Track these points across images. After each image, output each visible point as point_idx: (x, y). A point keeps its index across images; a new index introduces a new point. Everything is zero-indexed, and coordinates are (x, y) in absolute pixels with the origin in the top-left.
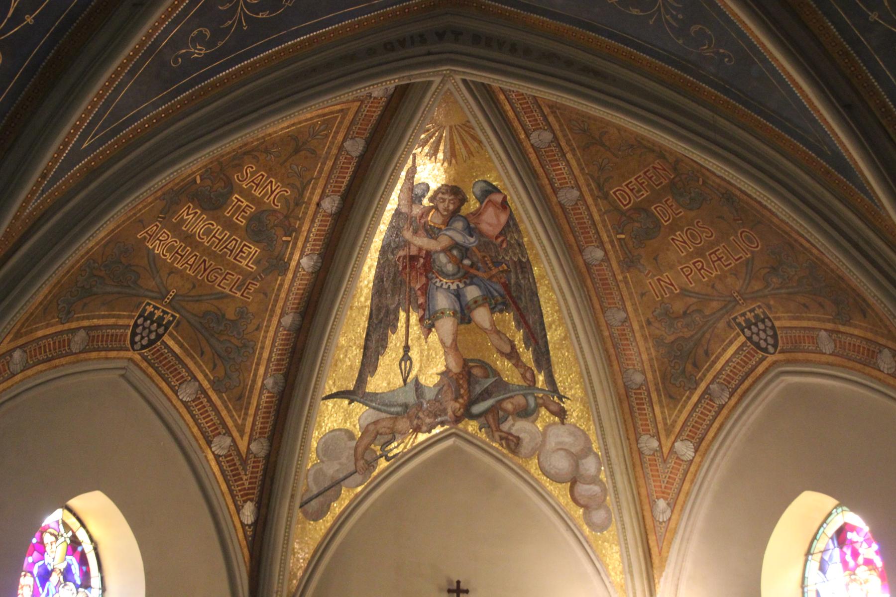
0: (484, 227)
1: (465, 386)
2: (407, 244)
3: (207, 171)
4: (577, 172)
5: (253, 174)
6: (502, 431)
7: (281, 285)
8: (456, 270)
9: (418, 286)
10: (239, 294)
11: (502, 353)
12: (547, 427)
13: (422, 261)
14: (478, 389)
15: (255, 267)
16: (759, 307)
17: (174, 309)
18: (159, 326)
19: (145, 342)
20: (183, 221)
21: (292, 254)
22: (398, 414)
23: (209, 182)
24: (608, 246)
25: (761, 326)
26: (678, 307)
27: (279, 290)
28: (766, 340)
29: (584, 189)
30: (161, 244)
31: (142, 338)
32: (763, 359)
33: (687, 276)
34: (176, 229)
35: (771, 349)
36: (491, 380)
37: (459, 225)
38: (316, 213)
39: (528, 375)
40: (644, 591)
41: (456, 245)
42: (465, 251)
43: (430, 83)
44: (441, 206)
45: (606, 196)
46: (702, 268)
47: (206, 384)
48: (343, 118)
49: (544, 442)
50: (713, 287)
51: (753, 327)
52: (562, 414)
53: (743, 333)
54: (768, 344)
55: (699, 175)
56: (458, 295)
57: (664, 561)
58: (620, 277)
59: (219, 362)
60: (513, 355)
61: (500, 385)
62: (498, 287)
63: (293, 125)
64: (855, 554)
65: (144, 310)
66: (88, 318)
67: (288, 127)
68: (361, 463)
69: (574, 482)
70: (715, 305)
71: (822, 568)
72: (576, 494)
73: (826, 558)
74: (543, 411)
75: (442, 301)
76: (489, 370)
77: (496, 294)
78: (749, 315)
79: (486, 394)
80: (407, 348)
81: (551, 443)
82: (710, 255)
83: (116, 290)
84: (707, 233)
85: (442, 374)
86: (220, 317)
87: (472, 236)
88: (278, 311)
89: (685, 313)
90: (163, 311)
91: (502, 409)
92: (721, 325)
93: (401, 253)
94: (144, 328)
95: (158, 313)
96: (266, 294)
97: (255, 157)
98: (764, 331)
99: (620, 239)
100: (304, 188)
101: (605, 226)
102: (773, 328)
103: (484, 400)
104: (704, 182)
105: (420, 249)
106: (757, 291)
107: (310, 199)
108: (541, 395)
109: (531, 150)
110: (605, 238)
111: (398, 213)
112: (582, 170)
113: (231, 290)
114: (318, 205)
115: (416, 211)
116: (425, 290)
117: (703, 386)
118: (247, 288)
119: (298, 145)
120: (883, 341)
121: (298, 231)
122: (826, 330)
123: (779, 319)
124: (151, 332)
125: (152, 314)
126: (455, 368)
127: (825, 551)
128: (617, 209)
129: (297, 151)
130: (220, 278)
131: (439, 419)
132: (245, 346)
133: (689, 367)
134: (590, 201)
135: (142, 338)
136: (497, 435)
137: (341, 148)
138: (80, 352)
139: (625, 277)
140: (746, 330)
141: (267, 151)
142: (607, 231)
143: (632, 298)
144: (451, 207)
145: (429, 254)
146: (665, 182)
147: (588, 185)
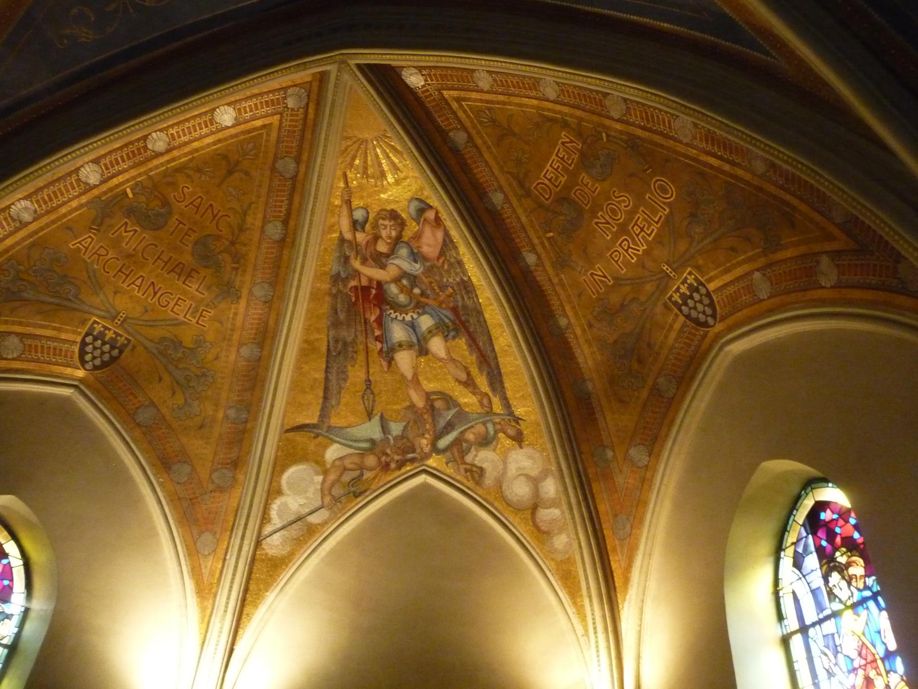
0: (426, 250)
1: (430, 420)
2: (357, 274)
3: (137, 184)
6: (466, 464)
7: (236, 314)
8: (408, 300)
9: (373, 318)
10: (194, 321)
11: (460, 382)
13: (374, 292)
14: (442, 423)
15: (206, 294)
16: (690, 273)
17: (129, 333)
18: (113, 347)
19: (98, 362)
25: (696, 296)
26: (615, 299)
31: (94, 358)
33: (616, 262)
35: (710, 321)
37: (404, 251)
39: (485, 401)
40: (604, 616)
41: (405, 274)
42: (414, 280)
45: (528, 194)
46: (629, 247)
49: (505, 472)
50: (643, 267)
51: (689, 301)
53: (681, 311)
54: (707, 316)
55: (600, 129)
57: (627, 580)
58: (555, 281)
60: (469, 383)
61: (462, 415)
62: (449, 313)
63: (219, 141)
64: (831, 537)
65: (92, 329)
66: (20, 324)
67: (214, 143)
68: (327, 499)
69: (534, 508)
70: (649, 288)
71: (798, 563)
72: (538, 520)
73: (800, 550)
74: (501, 435)
75: (398, 333)
76: (450, 401)
77: (447, 321)
78: (684, 289)
79: (449, 427)
80: (368, 382)
81: (512, 469)
82: (633, 228)
84: (624, 201)
86: (177, 344)
87: (416, 262)
89: (622, 305)
91: (466, 441)
92: (659, 309)
93: (353, 283)
94: (95, 348)
95: (109, 335)
96: (221, 322)
97: (188, 176)
98: (701, 302)
99: (549, 238)
102: (708, 295)
103: (448, 433)
104: (608, 136)
105: (370, 280)
106: (685, 252)
110: (536, 241)
113: (185, 317)
116: (380, 321)
117: (650, 382)
118: (201, 315)
122: (757, 270)
123: (710, 280)
127: (799, 540)
128: (541, 206)
129: (230, 173)
130: (172, 304)
131: (410, 456)
132: (204, 375)
133: (635, 366)
135: (94, 358)
138: (13, 359)
139: (561, 280)
140: (683, 308)
141: (199, 170)
144: (394, 234)
145: (380, 284)
147: (510, 185)
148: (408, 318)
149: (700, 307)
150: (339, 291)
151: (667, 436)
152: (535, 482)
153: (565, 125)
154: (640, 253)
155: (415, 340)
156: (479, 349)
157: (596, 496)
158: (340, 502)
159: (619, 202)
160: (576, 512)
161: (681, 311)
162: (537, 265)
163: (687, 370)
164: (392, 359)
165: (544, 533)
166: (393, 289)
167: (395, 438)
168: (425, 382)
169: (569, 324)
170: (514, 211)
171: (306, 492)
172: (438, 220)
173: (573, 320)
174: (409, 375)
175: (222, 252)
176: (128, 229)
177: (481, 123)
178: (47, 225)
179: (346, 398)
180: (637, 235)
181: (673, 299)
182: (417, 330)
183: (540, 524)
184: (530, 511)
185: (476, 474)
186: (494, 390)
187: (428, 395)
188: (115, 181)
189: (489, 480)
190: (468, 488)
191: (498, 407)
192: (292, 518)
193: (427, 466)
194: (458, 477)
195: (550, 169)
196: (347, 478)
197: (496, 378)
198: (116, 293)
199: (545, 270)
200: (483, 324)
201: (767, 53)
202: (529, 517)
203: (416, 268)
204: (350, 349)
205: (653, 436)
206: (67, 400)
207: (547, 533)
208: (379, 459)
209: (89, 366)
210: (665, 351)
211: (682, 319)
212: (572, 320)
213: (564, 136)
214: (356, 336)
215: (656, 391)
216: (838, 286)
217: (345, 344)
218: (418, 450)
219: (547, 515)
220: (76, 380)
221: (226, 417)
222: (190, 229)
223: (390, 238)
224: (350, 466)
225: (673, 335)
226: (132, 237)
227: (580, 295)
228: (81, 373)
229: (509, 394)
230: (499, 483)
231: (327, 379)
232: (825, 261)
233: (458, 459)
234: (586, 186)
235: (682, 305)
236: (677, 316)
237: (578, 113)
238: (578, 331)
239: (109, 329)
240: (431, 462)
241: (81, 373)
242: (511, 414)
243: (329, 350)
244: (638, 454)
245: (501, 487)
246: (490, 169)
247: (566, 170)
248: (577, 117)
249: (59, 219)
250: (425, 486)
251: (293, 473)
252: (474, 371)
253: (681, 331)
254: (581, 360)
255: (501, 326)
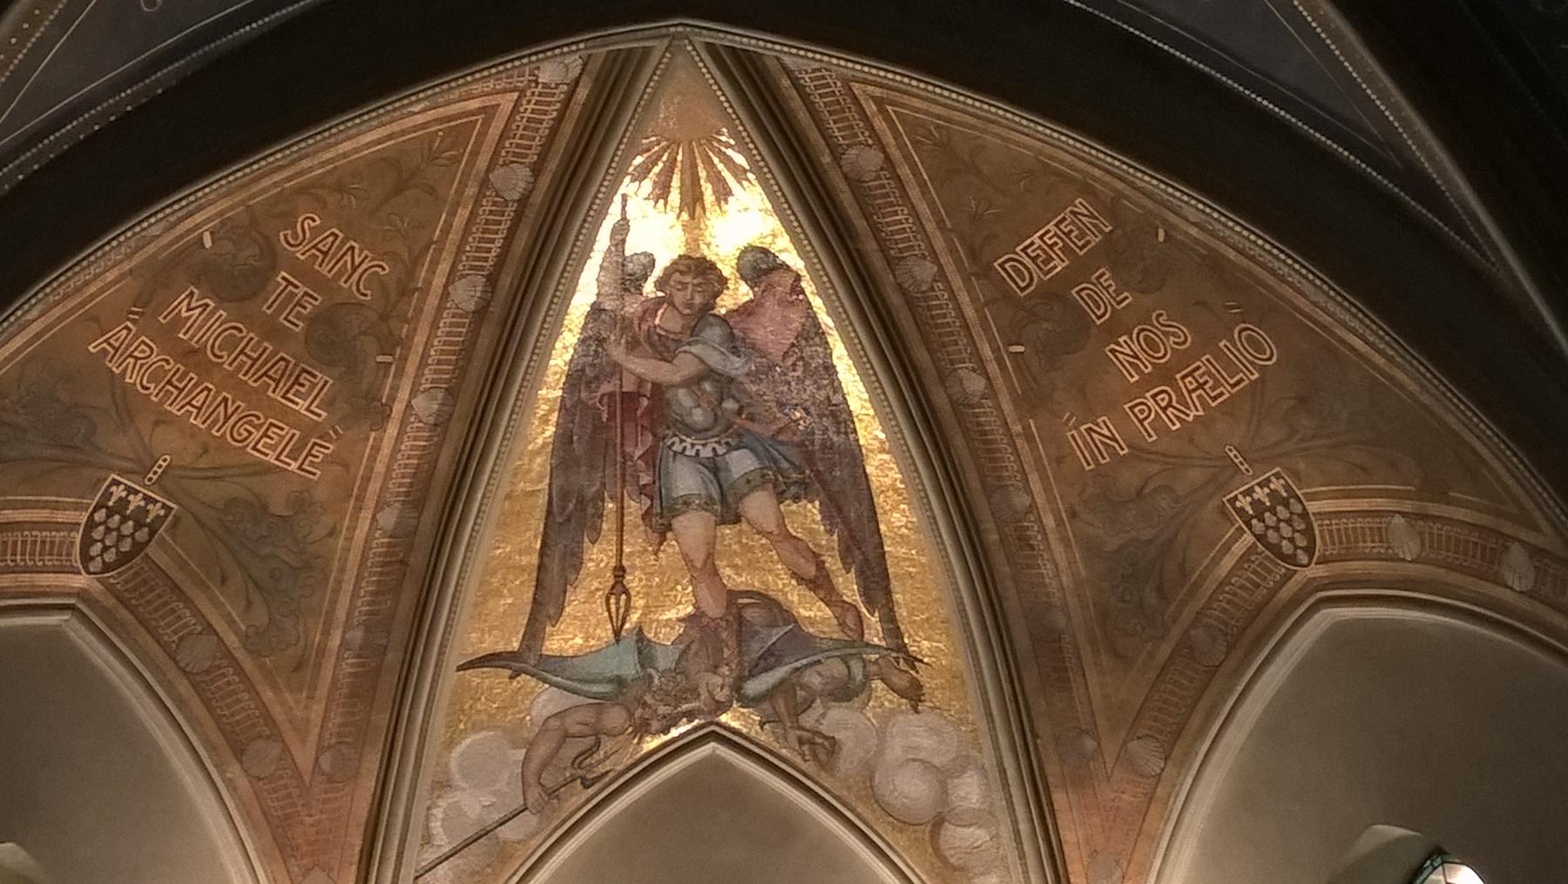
1: (732, 643)
2: (617, 369)
4: (930, 227)
5: (316, 231)
6: (803, 729)
7: (376, 449)
8: (710, 420)
9: (638, 453)
10: (294, 466)
11: (801, 579)
12: (888, 717)
13: (645, 402)
14: (755, 649)
15: (324, 414)
16: (1278, 476)
17: (170, 497)
18: (139, 525)
19: (110, 556)
20: (178, 322)
21: (395, 389)
22: (603, 696)
23: (228, 247)
24: (993, 368)
25: (1282, 512)
26: (1128, 479)
27: (372, 458)
28: (1292, 540)
29: (946, 259)
30: (134, 360)
31: (105, 549)
32: (1288, 576)
33: (1141, 422)
34: (166, 336)
36: (776, 634)
37: (714, 333)
38: (440, 309)
39: (850, 620)
41: (709, 374)
42: (726, 384)
43: (647, 52)
44: (679, 298)
45: (986, 272)
46: (1170, 405)
47: (232, 640)
48: (486, 124)
49: (880, 751)
50: (1191, 441)
51: (1267, 514)
52: (914, 694)
53: (1250, 526)
54: (1296, 548)
55: (1157, 223)
56: (714, 468)
58: (1017, 428)
59: (256, 598)
60: (819, 583)
61: (798, 639)
62: (793, 454)
65: (108, 495)
68: (534, 793)
69: (938, 823)
70: (1195, 475)
72: (943, 846)
74: (878, 684)
75: (686, 481)
76: (776, 610)
78: (1260, 494)
79: (769, 659)
80: (620, 572)
81: (895, 749)
82: (1183, 378)
83: (48, 452)
84: (1173, 334)
85: (688, 619)
86: (260, 509)
87: (735, 351)
88: (370, 502)
89: (1139, 492)
90: (146, 498)
91: (802, 687)
93: (606, 388)
94: (108, 530)
95: (136, 501)
96: (346, 466)
97: (318, 199)
98: (1289, 522)
100: (416, 261)
101: (986, 329)
102: (1304, 515)
103: (766, 670)
105: (641, 381)
106: (1277, 444)
107: (428, 283)
108: (873, 657)
109: (843, 186)
110: (987, 352)
111: (596, 310)
112: (940, 223)
113: (277, 459)
114: (445, 294)
115: (632, 307)
116: (652, 459)
117: (1176, 633)
118: (310, 454)
119: (405, 177)
120: (1508, 528)
121: (406, 343)
123: (1313, 497)
124: (121, 537)
125: (123, 502)
126: (714, 609)
128: (1008, 296)
129: (399, 189)
130: (256, 435)
131: (685, 707)
133: (1151, 598)
134: (957, 282)
135: (105, 549)
136: (793, 735)
137: (485, 183)
139: (1027, 428)
140: (1254, 521)
141: (340, 188)
142: (992, 340)
143: (1040, 469)
144: (698, 300)
145: (657, 387)
146: (1095, 241)
147: (952, 251)
148: (706, 453)
149: (1286, 530)
150: (580, 401)
151: (1202, 732)
152: (943, 778)
153: (1088, 191)
154: (1190, 419)
155: (715, 494)
156: (846, 522)
157: (1058, 815)
158: (557, 797)
159: (1166, 334)
160: (1028, 848)
161: (1250, 526)
162: (984, 397)
163: (1251, 627)
164: (669, 527)
165: (955, 869)
166: (684, 398)
167: (663, 674)
168: (728, 571)
169: (1033, 507)
170: (953, 297)
171: (494, 782)
172: (797, 289)
173: (1040, 500)
174: (699, 558)
175: (362, 333)
176: (193, 305)
177: (915, 144)
178: (60, 319)
179: (575, 604)
180: (1190, 392)
181: (1238, 504)
182: (722, 475)
183: (947, 854)
184: (929, 827)
185: (825, 749)
186: (870, 603)
187: (733, 595)
188: (189, 223)
189: (848, 762)
190: (805, 775)
191: (874, 633)
192: (471, 833)
193: (719, 724)
194: (784, 752)
195: (1038, 242)
196: (571, 750)
197: (876, 582)
198: (157, 423)
199: (998, 406)
200: (861, 480)
201: (1483, 255)
202: (927, 837)
203: (736, 366)
204: (590, 510)
205: (1176, 721)
206: (55, 634)
207: (961, 869)
208: (631, 715)
209: (96, 565)
210: (1210, 586)
211: (1248, 539)
212: (1039, 497)
213: (1081, 206)
214: (604, 485)
215: (1186, 647)
216: (1529, 594)
217: (581, 502)
218: (704, 695)
219: (960, 838)
220: (69, 595)
221: (345, 644)
222: (306, 294)
223: (690, 306)
224: (575, 729)
225: (1228, 562)
226: (196, 314)
227: (1059, 460)
228: (80, 581)
229: (902, 613)
230: (868, 772)
231: (541, 567)
232: (1517, 555)
233: (786, 718)
234: (1106, 288)
235: (1252, 517)
236: (1240, 531)
237: (1120, 185)
238: (1049, 521)
239: (136, 492)
240: (724, 718)
241: (80, 581)
242: (902, 648)
243: (549, 512)
244: (1145, 753)
245: (871, 779)
246: (917, 223)
247: (1066, 249)
248: (1114, 190)
249: (82, 305)
250: (713, 762)
251: (469, 746)
252: (833, 563)
253: (1244, 558)
254: (1047, 570)
255: (896, 490)
